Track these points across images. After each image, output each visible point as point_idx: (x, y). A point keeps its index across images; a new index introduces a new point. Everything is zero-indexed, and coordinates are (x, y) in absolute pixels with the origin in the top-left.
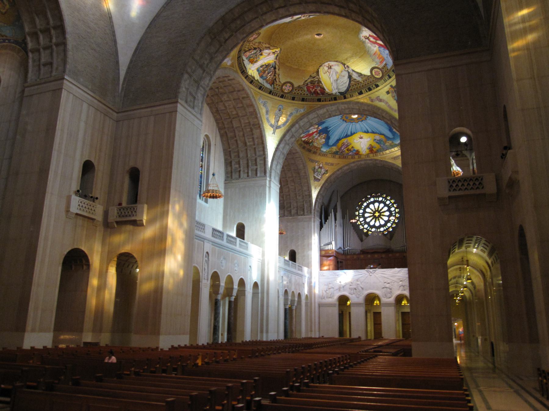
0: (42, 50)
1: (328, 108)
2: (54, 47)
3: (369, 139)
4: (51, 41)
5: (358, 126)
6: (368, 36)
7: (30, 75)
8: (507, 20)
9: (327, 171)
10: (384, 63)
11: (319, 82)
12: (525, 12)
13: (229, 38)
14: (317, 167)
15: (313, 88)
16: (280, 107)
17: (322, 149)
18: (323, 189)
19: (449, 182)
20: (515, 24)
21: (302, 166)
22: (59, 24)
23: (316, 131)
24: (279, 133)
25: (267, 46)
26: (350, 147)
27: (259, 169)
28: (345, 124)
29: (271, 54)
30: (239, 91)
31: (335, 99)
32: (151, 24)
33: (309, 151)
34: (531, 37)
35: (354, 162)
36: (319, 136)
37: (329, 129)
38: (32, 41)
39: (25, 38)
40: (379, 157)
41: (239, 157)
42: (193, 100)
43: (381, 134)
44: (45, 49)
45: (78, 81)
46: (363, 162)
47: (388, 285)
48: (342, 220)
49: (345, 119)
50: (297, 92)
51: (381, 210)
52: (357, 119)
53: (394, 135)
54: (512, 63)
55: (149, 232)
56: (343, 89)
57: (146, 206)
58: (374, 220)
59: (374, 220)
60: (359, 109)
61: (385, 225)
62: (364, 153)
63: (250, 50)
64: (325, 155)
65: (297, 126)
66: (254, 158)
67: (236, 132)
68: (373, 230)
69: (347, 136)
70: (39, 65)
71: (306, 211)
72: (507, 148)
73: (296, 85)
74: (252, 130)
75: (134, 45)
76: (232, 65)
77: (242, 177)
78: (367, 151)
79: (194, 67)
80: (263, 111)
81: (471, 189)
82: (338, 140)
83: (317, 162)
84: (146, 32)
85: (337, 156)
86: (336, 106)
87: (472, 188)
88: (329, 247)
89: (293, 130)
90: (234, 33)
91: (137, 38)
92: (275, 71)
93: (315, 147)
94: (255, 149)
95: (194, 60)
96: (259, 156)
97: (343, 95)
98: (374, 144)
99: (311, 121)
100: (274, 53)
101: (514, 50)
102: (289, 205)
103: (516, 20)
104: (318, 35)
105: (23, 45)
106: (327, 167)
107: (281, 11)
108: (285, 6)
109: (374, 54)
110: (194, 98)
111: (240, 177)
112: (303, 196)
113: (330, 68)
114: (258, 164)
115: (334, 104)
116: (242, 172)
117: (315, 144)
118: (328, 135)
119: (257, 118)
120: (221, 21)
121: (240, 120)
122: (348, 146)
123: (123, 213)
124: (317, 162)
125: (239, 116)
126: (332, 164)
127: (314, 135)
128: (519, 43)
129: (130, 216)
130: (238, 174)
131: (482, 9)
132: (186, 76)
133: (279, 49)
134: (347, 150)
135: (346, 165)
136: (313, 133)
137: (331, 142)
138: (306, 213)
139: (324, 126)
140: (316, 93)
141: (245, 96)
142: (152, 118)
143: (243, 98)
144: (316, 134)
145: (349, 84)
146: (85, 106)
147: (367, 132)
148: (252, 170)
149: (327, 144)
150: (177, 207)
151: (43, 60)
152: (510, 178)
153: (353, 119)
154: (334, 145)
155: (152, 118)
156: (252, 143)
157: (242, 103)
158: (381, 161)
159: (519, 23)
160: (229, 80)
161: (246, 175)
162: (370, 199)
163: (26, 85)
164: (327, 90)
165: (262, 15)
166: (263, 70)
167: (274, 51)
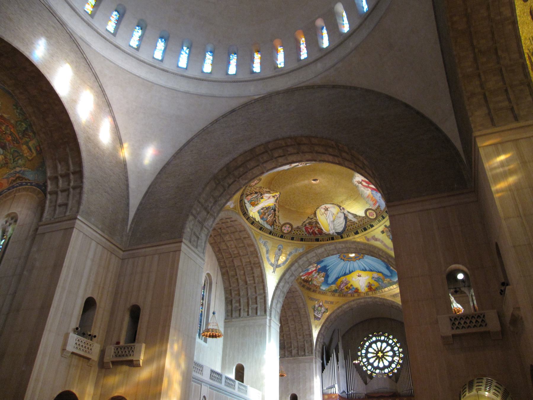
0: (59, 193)
1: (326, 247)
2: (71, 190)
3: (367, 277)
4: (69, 185)
5: (356, 264)
6: (361, 181)
7: (45, 215)
8: (487, 165)
9: (327, 309)
10: (377, 205)
11: (317, 223)
12: (502, 158)
13: (233, 183)
14: (317, 306)
15: (311, 229)
16: (280, 246)
17: (321, 288)
18: (324, 328)
19: (451, 320)
20: (495, 168)
21: (302, 304)
22: (78, 169)
24: (279, 272)
25: (268, 190)
26: (349, 285)
27: (259, 308)
28: (342, 263)
29: (271, 197)
30: (240, 231)
31: (333, 239)
32: (161, 170)
33: (309, 289)
34: (512, 180)
35: (353, 300)
36: (318, 274)
37: (328, 268)
38: (51, 184)
39: (46, 182)
40: (378, 295)
41: (239, 296)
42: (196, 239)
43: (379, 272)
44: (63, 191)
45: (89, 221)
46: (362, 300)
48: (344, 361)
49: (343, 258)
50: (296, 232)
51: (384, 350)
52: (355, 257)
54: (498, 203)
55: (145, 373)
56: (340, 229)
57: (144, 345)
58: (377, 361)
59: (377, 361)
60: (356, 248)
61: (390, 366)
62: (363, 291)
63: (251, 194)
64: (324, 293)
65: (296, 264)
66: (254, 297)
67: (237, 271)
68: (378, 371)
69: (345, 274)
70: (55, 206)
71: (307, 351)
72: (505, 284)
73: (295, 226)
74: (252, 269)
75: (144, 189)
76: (235, 208)
77: (242, 315)
78: (366, 289)
79: (198, 210)
80: (263, 250)
81: (474, 327)
83: (316, 300)
84: (157, 178)
85: (337, 294)
86: (333, 245)
87: (475, 326)
88: (332, 391)
89: (293, 268)
90: (237, 179)
91: (149, 183)
92: (275, 213)
93: (315, 286)
94: (255, 287)
95: (199, 202)
96: (260, 295)
97: (340, 235)
98: (372, 282)
99: (310, 260)
100: (274, 197)
101: (498, 191)
102: (289, 345)
103: (496, 165)
104: (315, 180)
105: (43, 188)
106: (327, 306)
107: (280, 160)
108: (284, 156)
109: (368, 197)
110: (198, 238)
111: (240, 316)
112: (304, 336)
113: (326, 209)
114: (258, 303)
115: (332, 244)
116: (242, 311)
117: (315, 283)
119: (257, 257)
120: (225, 169)
121: (241, 259)
122: (347, 284)
123: (120, 352)
125: (240, 256)
126: (332, 303)
127: (314, 273)
128: (502, 185)
129: (127, 355)
130: (238, 312)
131: (463, 157)
132: (191, 218)
133: (279, 193)
134: (347, 288)
135: (346, 304)
136: (312, 272)
137: (330, 280)
138: (307, 354)
139: (323, 264)
140: (314, 233)
141: (247, 236)
142: (156, 257)
143: (245, 238)
144: (315, 273)
145: (345, 225)
146: (94, 244)
147: (365, 270)
148: (252, 309)
149: (326, 282)
150: (176, 347)
151: (60, 201)
152: (513, 315)
153: (351, 258)
154: (333, 283)
155: (156, 257)
156: (252, 282)
157: (243, 243)
158: (381, 299)
159: (498, 167)
160: (232, 221)
161: (246, 314)
162: (371, 338)
163: (41, 223)
164: (324, 230)
165: (263, 163)
166: (263, 213)
167: (273, 195)
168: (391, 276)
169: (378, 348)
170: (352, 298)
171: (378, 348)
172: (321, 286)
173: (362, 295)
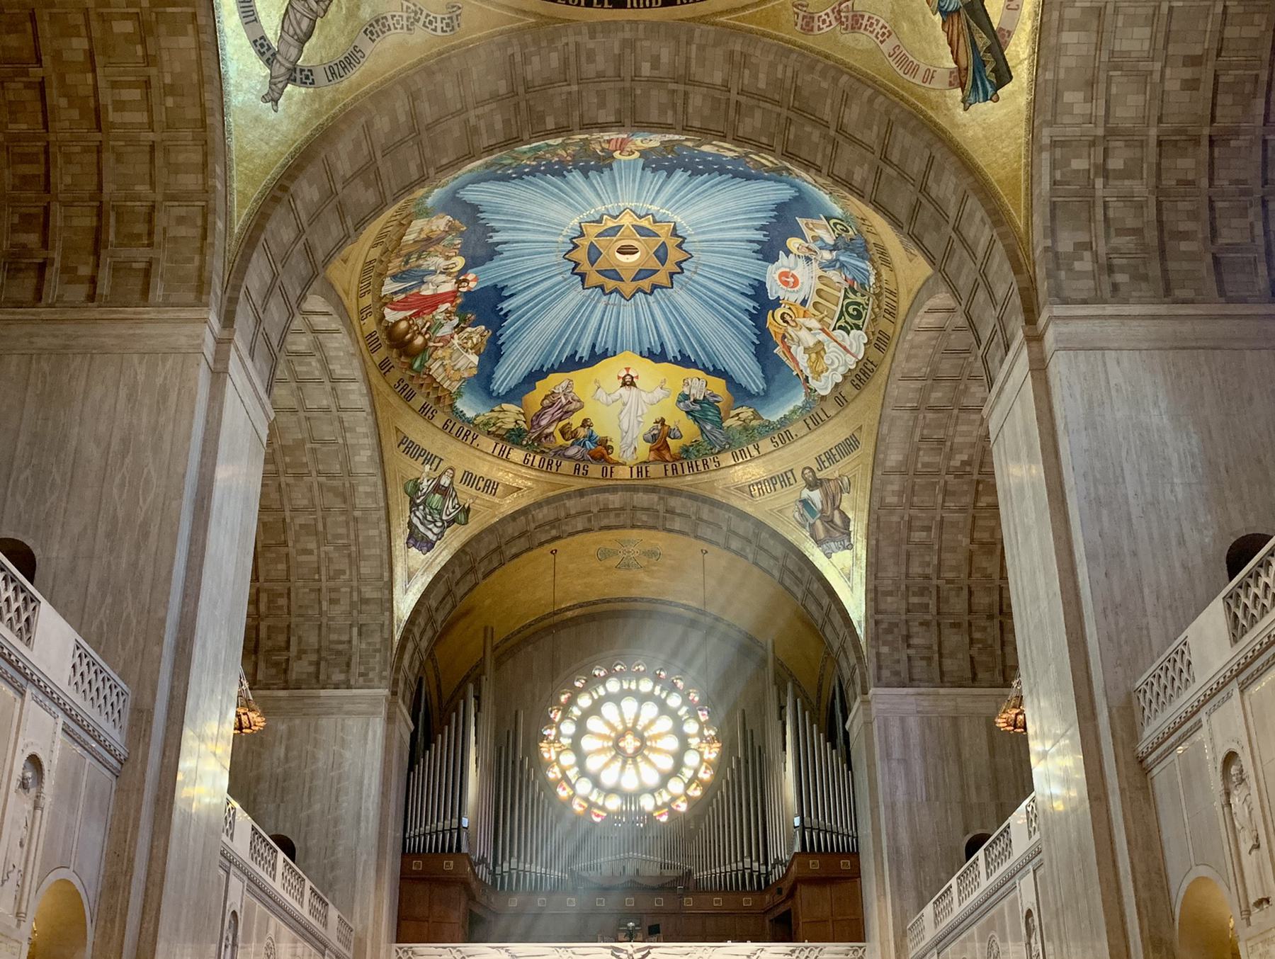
14: (425, 485)
17: (459, 405)
23: (453, 295)
26: (575, 421)
28: (576, 295)
35: (581, 493)
36: (459, 329)
49: (585, 267)
53: (768, 379)
64: (463, 430)
69: (573, 363)
83: (429, 459)
85: (517, 455)
102: (281, 639)
118: (494, 338)
122: (568, 413)
124: (429, 459)
134: (563, 433)
135: (548, 501)
136: (435, 301)
137: (507, 374)
147: (658, 356)
149: (483, 382)
154: (515, 394)
162: (603, 681)
168: (765, 397)
169: (623, 721)
171: (623, 721)
172: (459, 394)
173: (623, 473)
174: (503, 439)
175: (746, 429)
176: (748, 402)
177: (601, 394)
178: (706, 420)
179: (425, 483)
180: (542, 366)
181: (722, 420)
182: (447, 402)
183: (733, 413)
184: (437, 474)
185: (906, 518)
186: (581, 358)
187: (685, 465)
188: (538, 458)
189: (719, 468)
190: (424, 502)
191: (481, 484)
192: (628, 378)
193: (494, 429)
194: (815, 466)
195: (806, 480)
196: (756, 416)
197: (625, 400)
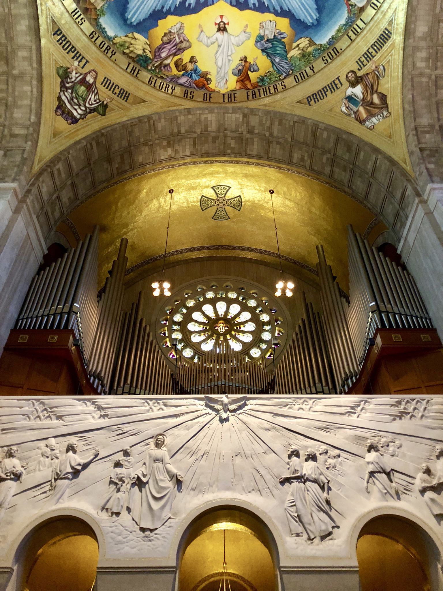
17: (103, 21)
47: (308, 468)
53: (320, 9)
78: (232, 83)
82: (157, 15)
83: (78, 56)
85: (145, 75)
124: (78, 56)
134: (177, 65)
170: (187, 104)
174: (133, 61)
175: (304, 56)
176: (306, 33)
177: (203, 37)
178: (275, 54)
179: (74, 73)
180: (163, 7)
181: (287, 53)
182: (94, 17)
183: (295, 45)
184: (85, 71)
185: (433, 77)
186: (190, 5)
187: (261, 91)
188: (159, 81)
189: (285, 88)
190: (72, 88)
191: (117, 91)
192: (222, 25)
193: (127, 51)
194: (355, 67)
195: (349, 81)
196: (312, 43)
197: (220, 42)
